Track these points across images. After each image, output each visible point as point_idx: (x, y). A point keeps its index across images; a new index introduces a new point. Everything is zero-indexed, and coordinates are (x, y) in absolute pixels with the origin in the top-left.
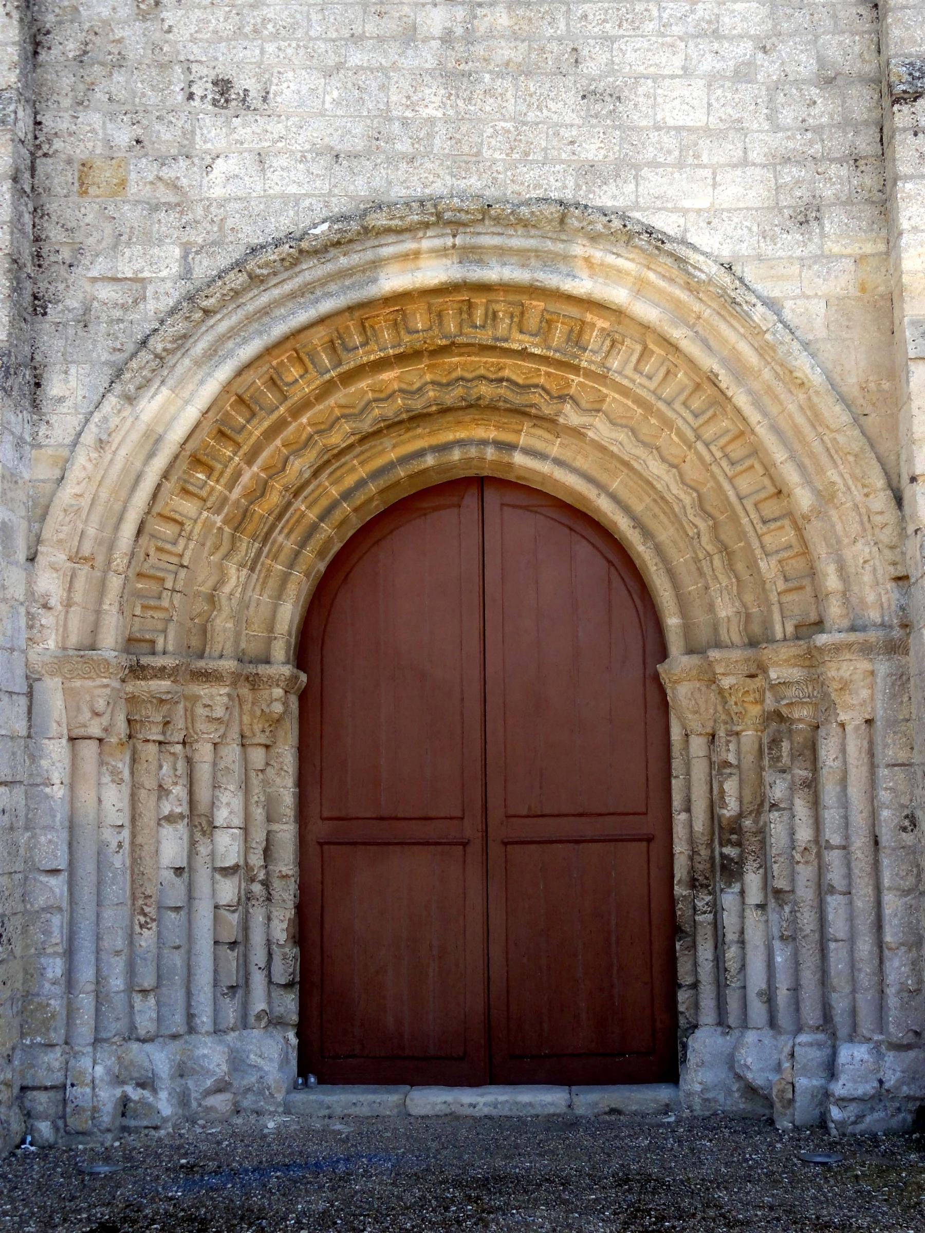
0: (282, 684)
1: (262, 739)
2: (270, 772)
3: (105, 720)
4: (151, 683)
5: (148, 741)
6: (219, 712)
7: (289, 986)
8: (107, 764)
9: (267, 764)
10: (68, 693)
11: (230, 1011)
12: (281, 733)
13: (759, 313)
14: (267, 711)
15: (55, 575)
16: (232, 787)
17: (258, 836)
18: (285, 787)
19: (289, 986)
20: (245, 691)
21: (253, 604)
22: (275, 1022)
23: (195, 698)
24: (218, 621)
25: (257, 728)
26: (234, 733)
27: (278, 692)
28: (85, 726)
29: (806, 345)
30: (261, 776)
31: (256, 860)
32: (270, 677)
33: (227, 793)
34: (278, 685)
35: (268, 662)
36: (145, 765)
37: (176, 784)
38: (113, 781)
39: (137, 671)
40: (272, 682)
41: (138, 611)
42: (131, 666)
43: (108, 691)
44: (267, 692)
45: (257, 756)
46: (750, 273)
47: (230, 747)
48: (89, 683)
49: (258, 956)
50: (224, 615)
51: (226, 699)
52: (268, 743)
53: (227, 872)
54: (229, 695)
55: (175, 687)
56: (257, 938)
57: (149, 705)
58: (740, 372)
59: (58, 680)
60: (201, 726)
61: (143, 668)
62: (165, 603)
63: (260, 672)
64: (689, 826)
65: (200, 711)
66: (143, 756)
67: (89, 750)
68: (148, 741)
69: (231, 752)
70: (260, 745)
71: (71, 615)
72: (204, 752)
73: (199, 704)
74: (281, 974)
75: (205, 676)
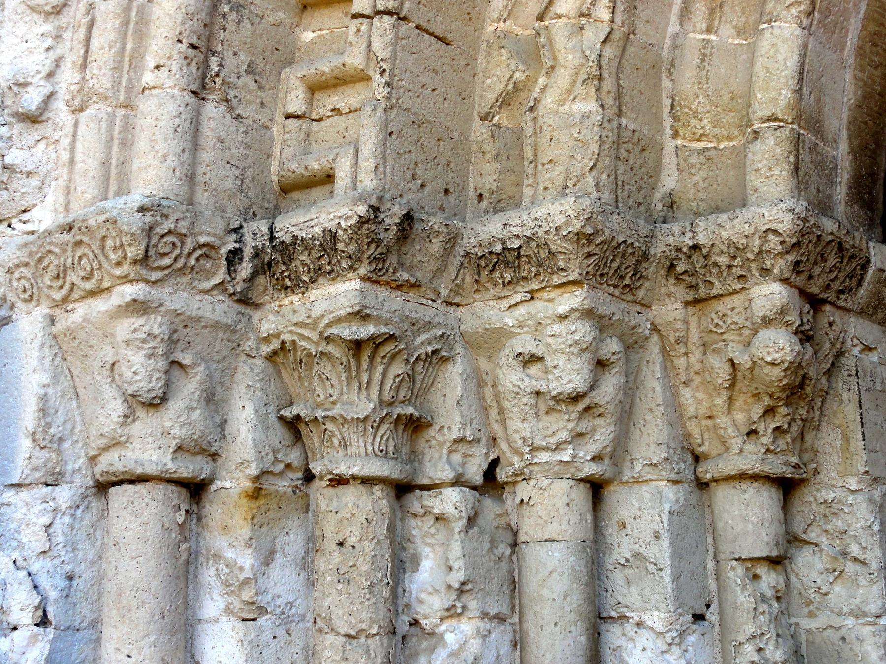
0: (781, 266)
1: (750, 457)
2: (809, 566)
3: (181, 417)
4: (313, 294)
5: (339, 481)
6: (568, 374)
8: (217, 557)
9: (793, 540)
10: (61, 345)
12: (828, 440)
14: (743, 360)
15: (48, 27)
16: (656, 619)
18: (859, 614)
20: (670, 309)
21: (692, 58)
23: (493, 340)
24: (549, 101)
25: (731, 424)
26: (651, 443)
27: (769, 294)
28: (115, 444)
30: (769, 579)
32: (736, 250)
33: (645, 638)
34: (765, 272)
36: (336, 557)
37: (451, 613)
38: (229, 611)
39: (279, 266)
40: (745, 263)
41: (296, 102)
42: (257, 253)
43: (156, 324)
44: (737, 301)
45: (747, 518)
47: (645, 491)
48: (101, 306)
50: (563, 78)
51: (583, 331)
52: (776, 467)
54: (588, 314)
55: (391, 303)
57: (327, 369)
59: (41, 311)
60: (521, 427)
61: (286, 250)
62: (355, 59)
63: (702, 239)
65: (513, 378)
66: (330, 529)
67: (138, 516)
68: (339, 481)
69: (646, 511)
70: (742, 476)
71: (82, 129)
72: (549, 510)
73: (506, 356)
75: (508, 264)
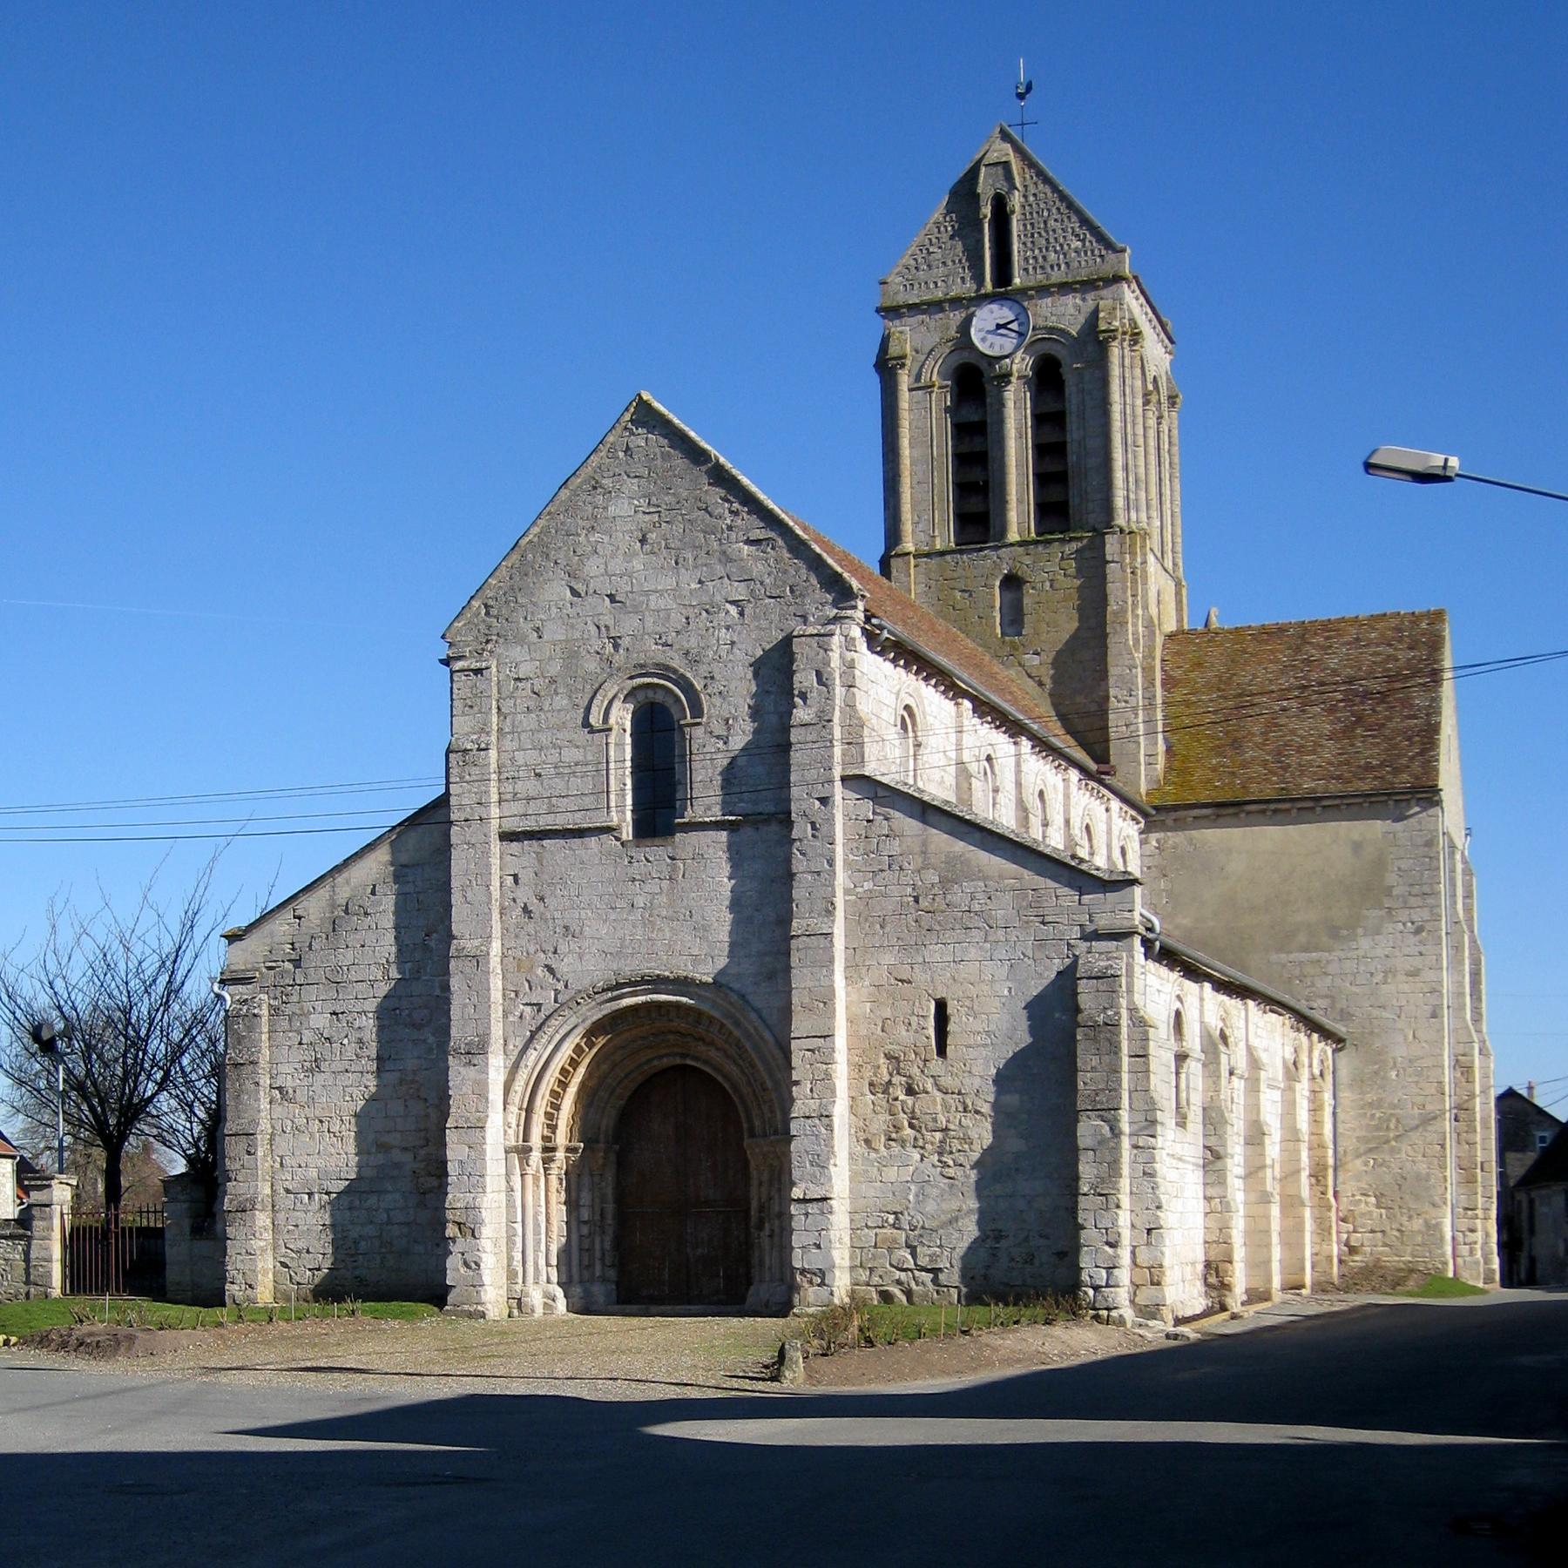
7: (613, 1266)
11: (586, 1274)
13: (753, 1016)
17: (597, 1209)
19: (613, 1266)
22: (604, 1279)
29: (768, 1026)
31: (597, 1217)
35: (597, 1142)
45: (597, 1179)
46: (750, 997)
49: (598, 1254)
53: (585, 1222)
56: (597, 1246)
58: (749, 1036)
64: (754, 1204)
74: (608, 1261)
